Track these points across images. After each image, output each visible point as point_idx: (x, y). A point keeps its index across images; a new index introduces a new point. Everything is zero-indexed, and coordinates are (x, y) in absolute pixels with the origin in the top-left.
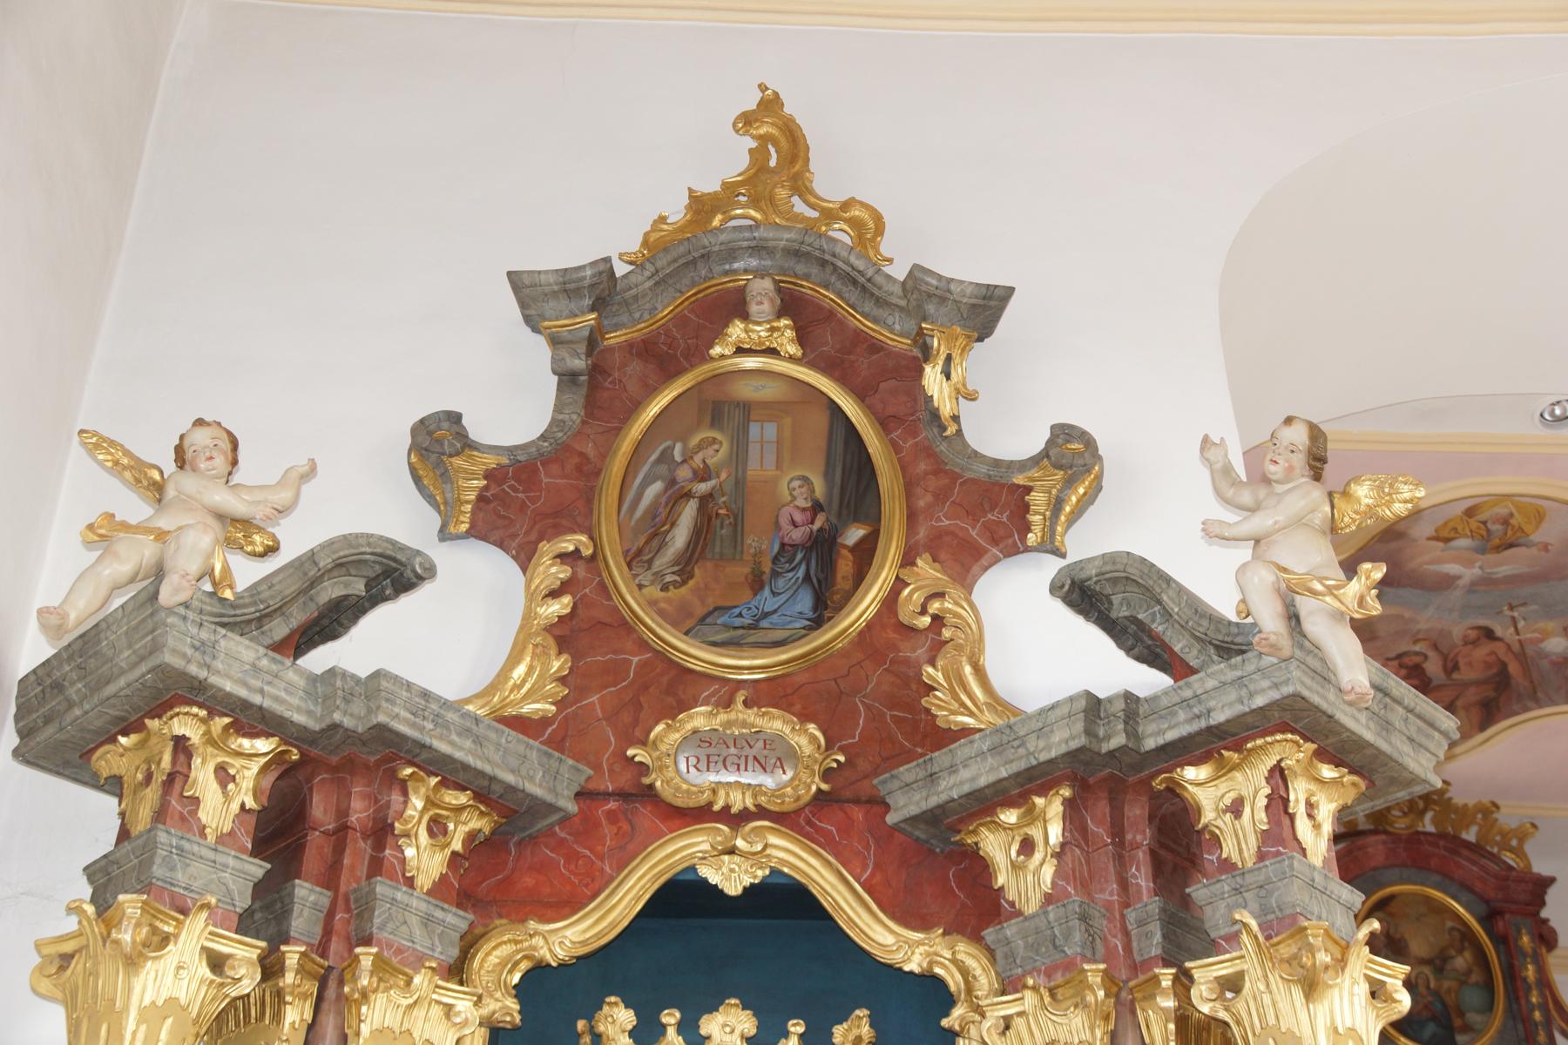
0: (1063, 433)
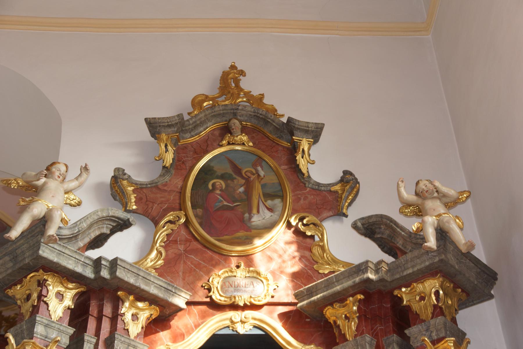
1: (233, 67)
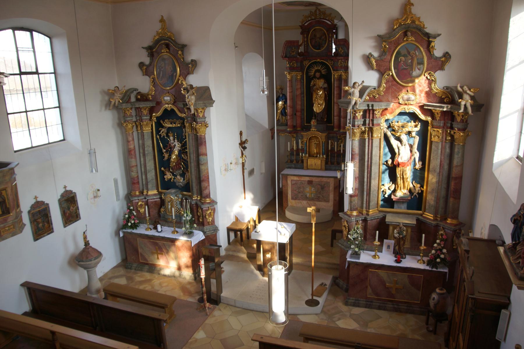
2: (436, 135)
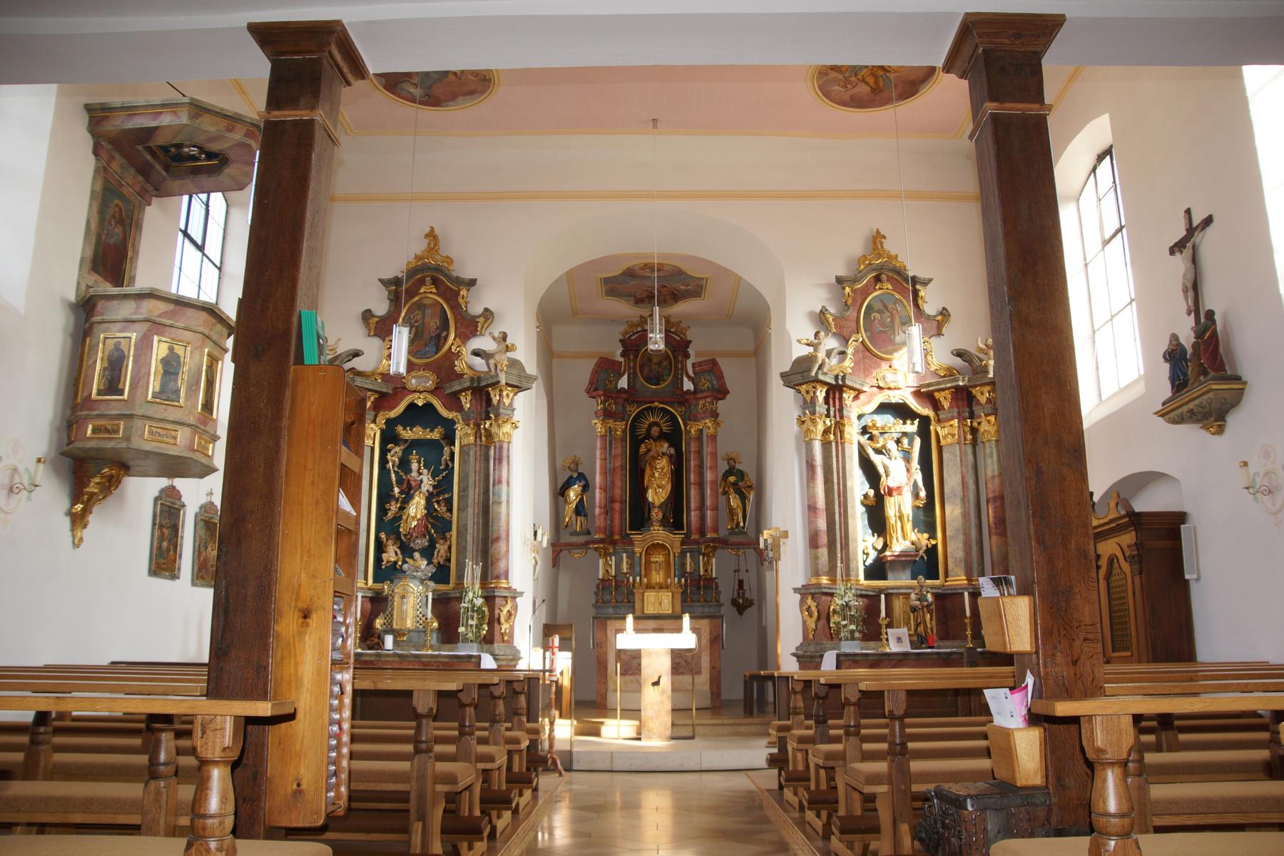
0: (486, 310)
1: (878, 232)
2: (948, 431)
